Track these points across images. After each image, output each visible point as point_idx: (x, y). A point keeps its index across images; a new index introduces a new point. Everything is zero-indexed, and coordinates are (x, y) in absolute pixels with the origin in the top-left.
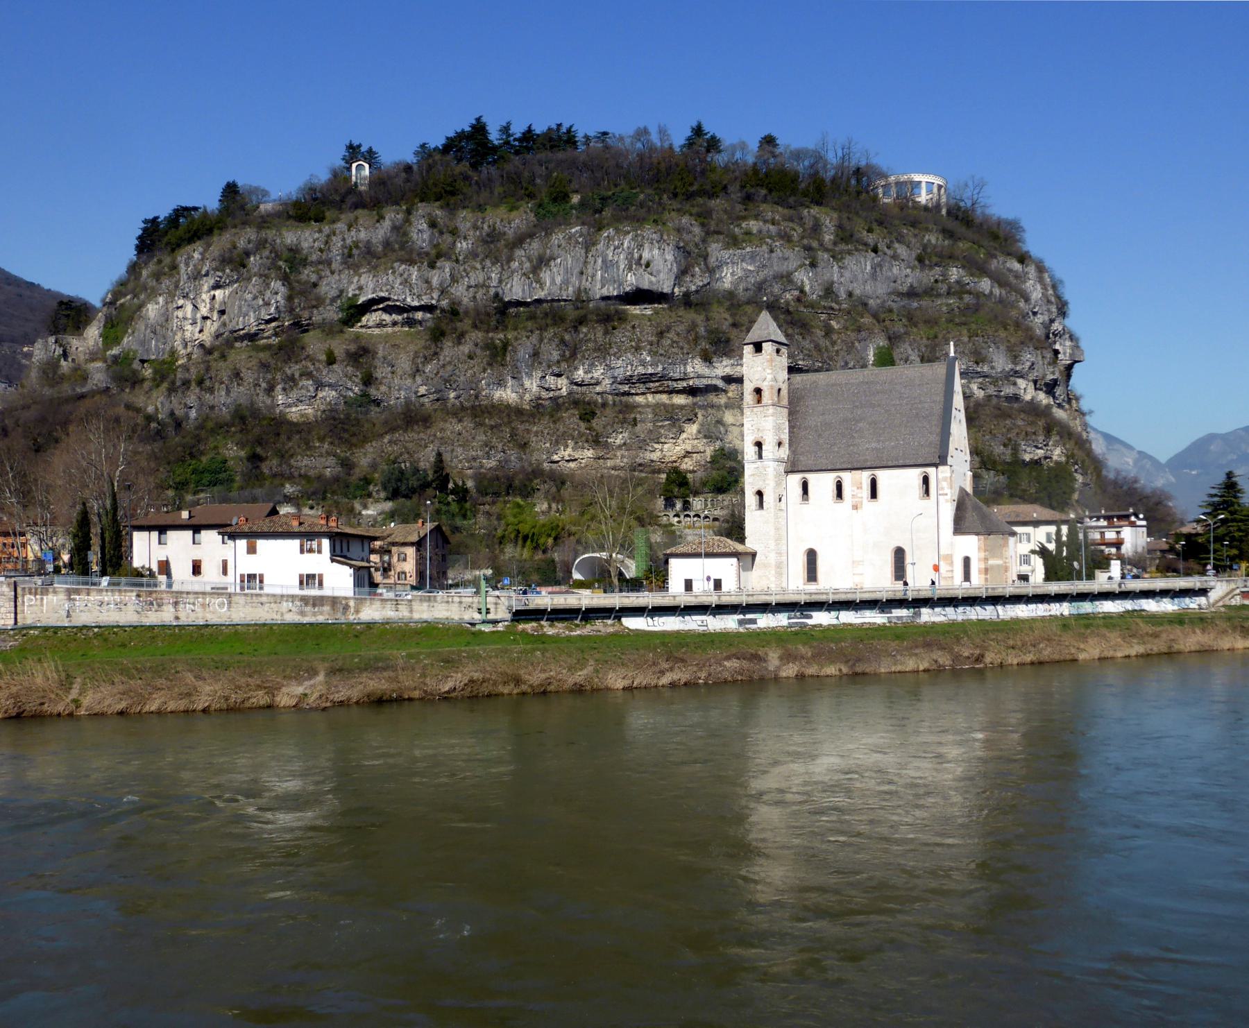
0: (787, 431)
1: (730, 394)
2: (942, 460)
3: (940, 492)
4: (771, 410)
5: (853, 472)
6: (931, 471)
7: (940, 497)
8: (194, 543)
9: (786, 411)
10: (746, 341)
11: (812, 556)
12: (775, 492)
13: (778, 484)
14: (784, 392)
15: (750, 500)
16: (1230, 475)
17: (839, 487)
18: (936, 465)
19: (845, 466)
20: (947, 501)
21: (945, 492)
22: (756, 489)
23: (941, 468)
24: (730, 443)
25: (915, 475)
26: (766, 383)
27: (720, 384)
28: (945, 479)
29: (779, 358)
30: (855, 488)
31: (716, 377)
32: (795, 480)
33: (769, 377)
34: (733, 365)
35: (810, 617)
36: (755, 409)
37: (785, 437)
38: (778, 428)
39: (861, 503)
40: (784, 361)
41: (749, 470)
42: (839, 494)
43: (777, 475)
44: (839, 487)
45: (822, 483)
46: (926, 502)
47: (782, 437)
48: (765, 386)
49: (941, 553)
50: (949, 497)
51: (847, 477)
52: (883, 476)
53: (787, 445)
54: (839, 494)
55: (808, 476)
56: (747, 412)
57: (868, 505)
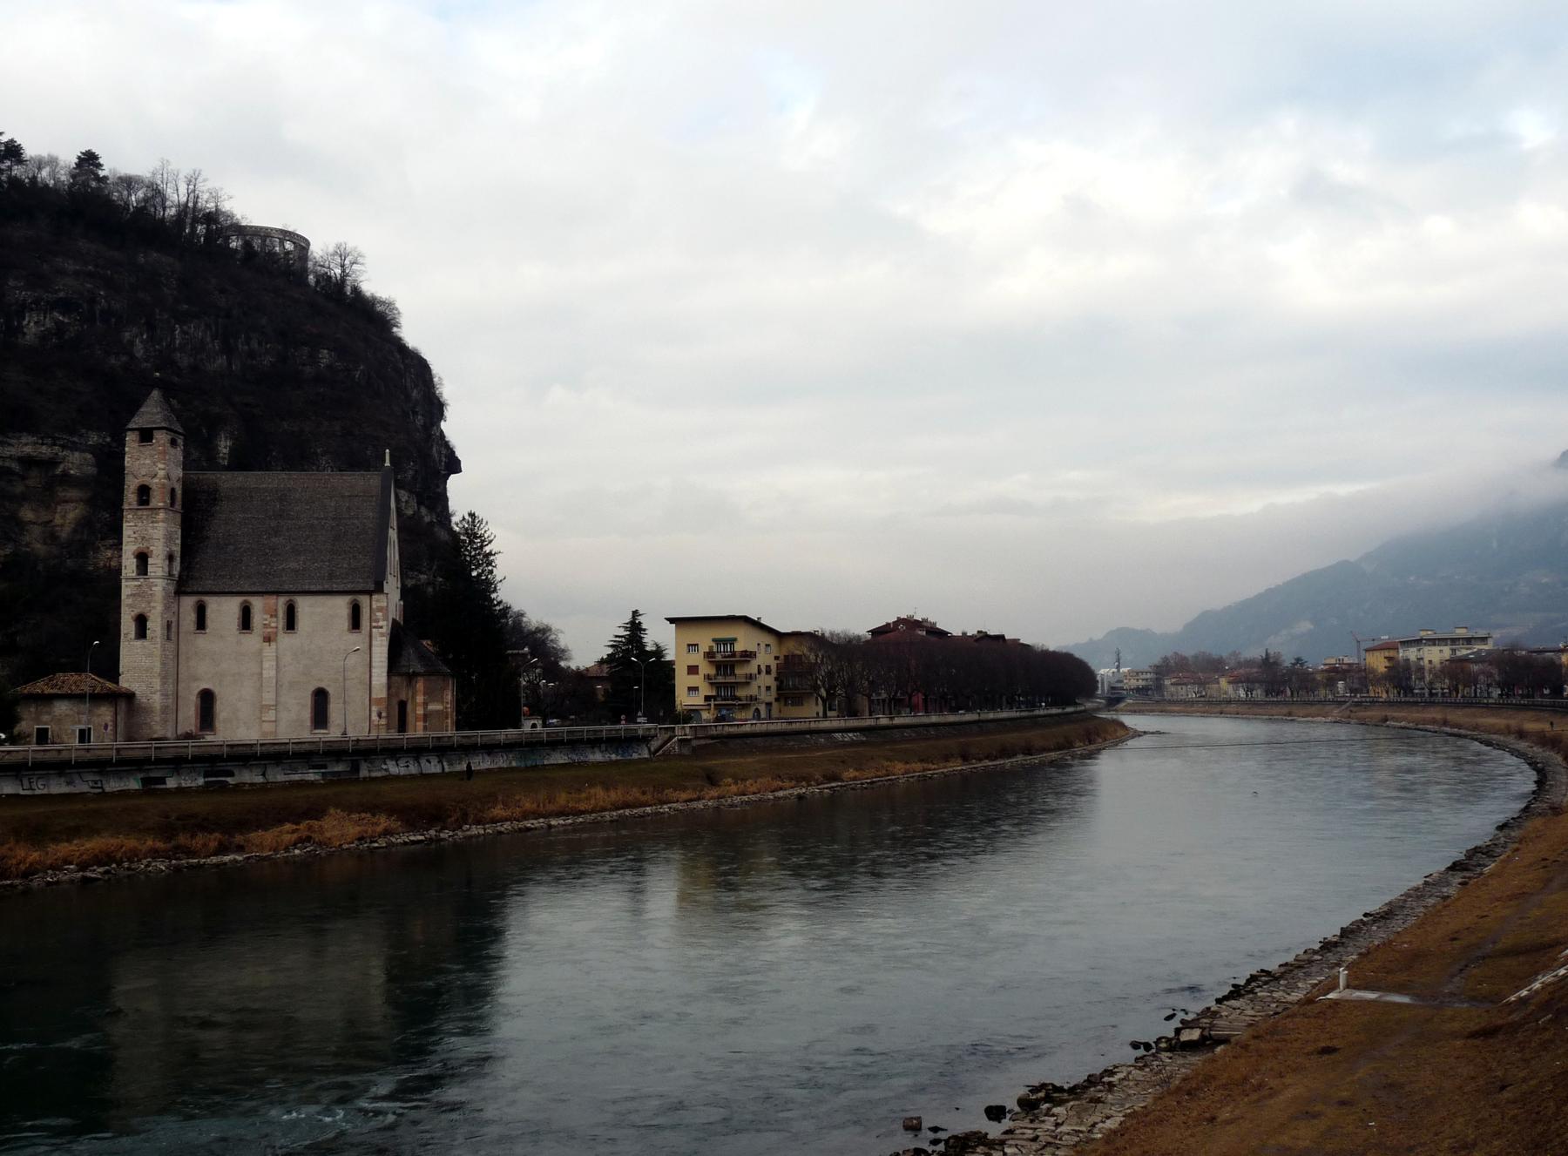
0: (179, 542)
1: (31, 483)
2: (379, 589)
3: (374, 624)
4: (162, 515)
5: (266, 597)
6: (364, 600)
7: (374, 630)
8: (689, 645)
9: (178, 518)
10: (131, 425)
11: (207, 698)
12: (163, 618)
13: (167, 608)
14: (179, 492)
15: (127, 626)
16: (635, 613)
17: (246, 614)
18: (370, 593)
19: (254, 589)
20: (382, 635)
21: (381, 624)
22: (137, 611)
23: (375, 597)
24: (27, 545)
25: (341, 605)
26: (156, 480)
27: (15, 466)
28: (380, 609)
29: (172, 451)
30: (268, 616)
31: (11, 457)
32: (189, 602)
33: (161, 473)
34: (35, 443)
35: (231, 774)
36: (140, 513)
37: (177, 549)
38: (169, 538)
39: (276, 634)
40: (178, 454)
41: (127, 589)
42: (246, 623)
43: (167, 596)
44: (246, 614)
45: (224, 610)
46: (354, 637)
47: (174, 548)
48: (154, 483)
49: (374, 696)
50: (383, 630)
51: (257, 604)
52: (304, 605)
53: (179, 559)
54: (246, 623)
55: (206, 599)
56: (128, 516)
57: (286, 640)
